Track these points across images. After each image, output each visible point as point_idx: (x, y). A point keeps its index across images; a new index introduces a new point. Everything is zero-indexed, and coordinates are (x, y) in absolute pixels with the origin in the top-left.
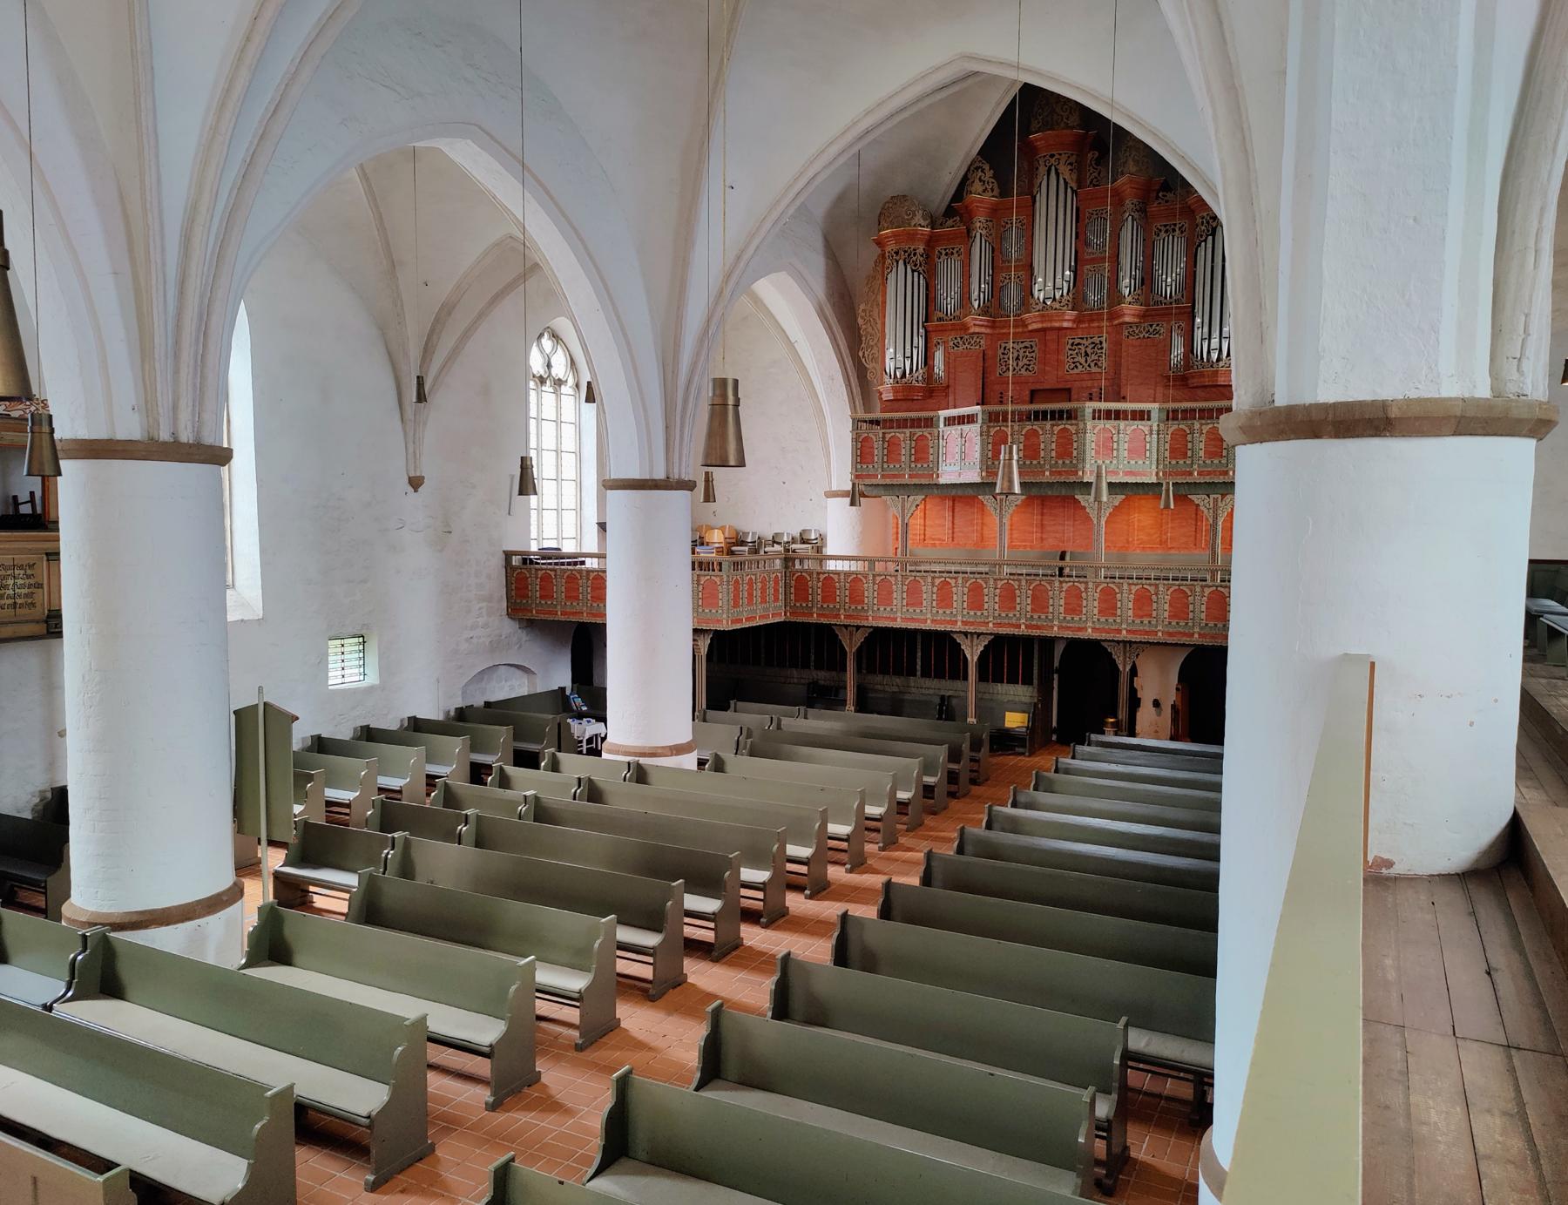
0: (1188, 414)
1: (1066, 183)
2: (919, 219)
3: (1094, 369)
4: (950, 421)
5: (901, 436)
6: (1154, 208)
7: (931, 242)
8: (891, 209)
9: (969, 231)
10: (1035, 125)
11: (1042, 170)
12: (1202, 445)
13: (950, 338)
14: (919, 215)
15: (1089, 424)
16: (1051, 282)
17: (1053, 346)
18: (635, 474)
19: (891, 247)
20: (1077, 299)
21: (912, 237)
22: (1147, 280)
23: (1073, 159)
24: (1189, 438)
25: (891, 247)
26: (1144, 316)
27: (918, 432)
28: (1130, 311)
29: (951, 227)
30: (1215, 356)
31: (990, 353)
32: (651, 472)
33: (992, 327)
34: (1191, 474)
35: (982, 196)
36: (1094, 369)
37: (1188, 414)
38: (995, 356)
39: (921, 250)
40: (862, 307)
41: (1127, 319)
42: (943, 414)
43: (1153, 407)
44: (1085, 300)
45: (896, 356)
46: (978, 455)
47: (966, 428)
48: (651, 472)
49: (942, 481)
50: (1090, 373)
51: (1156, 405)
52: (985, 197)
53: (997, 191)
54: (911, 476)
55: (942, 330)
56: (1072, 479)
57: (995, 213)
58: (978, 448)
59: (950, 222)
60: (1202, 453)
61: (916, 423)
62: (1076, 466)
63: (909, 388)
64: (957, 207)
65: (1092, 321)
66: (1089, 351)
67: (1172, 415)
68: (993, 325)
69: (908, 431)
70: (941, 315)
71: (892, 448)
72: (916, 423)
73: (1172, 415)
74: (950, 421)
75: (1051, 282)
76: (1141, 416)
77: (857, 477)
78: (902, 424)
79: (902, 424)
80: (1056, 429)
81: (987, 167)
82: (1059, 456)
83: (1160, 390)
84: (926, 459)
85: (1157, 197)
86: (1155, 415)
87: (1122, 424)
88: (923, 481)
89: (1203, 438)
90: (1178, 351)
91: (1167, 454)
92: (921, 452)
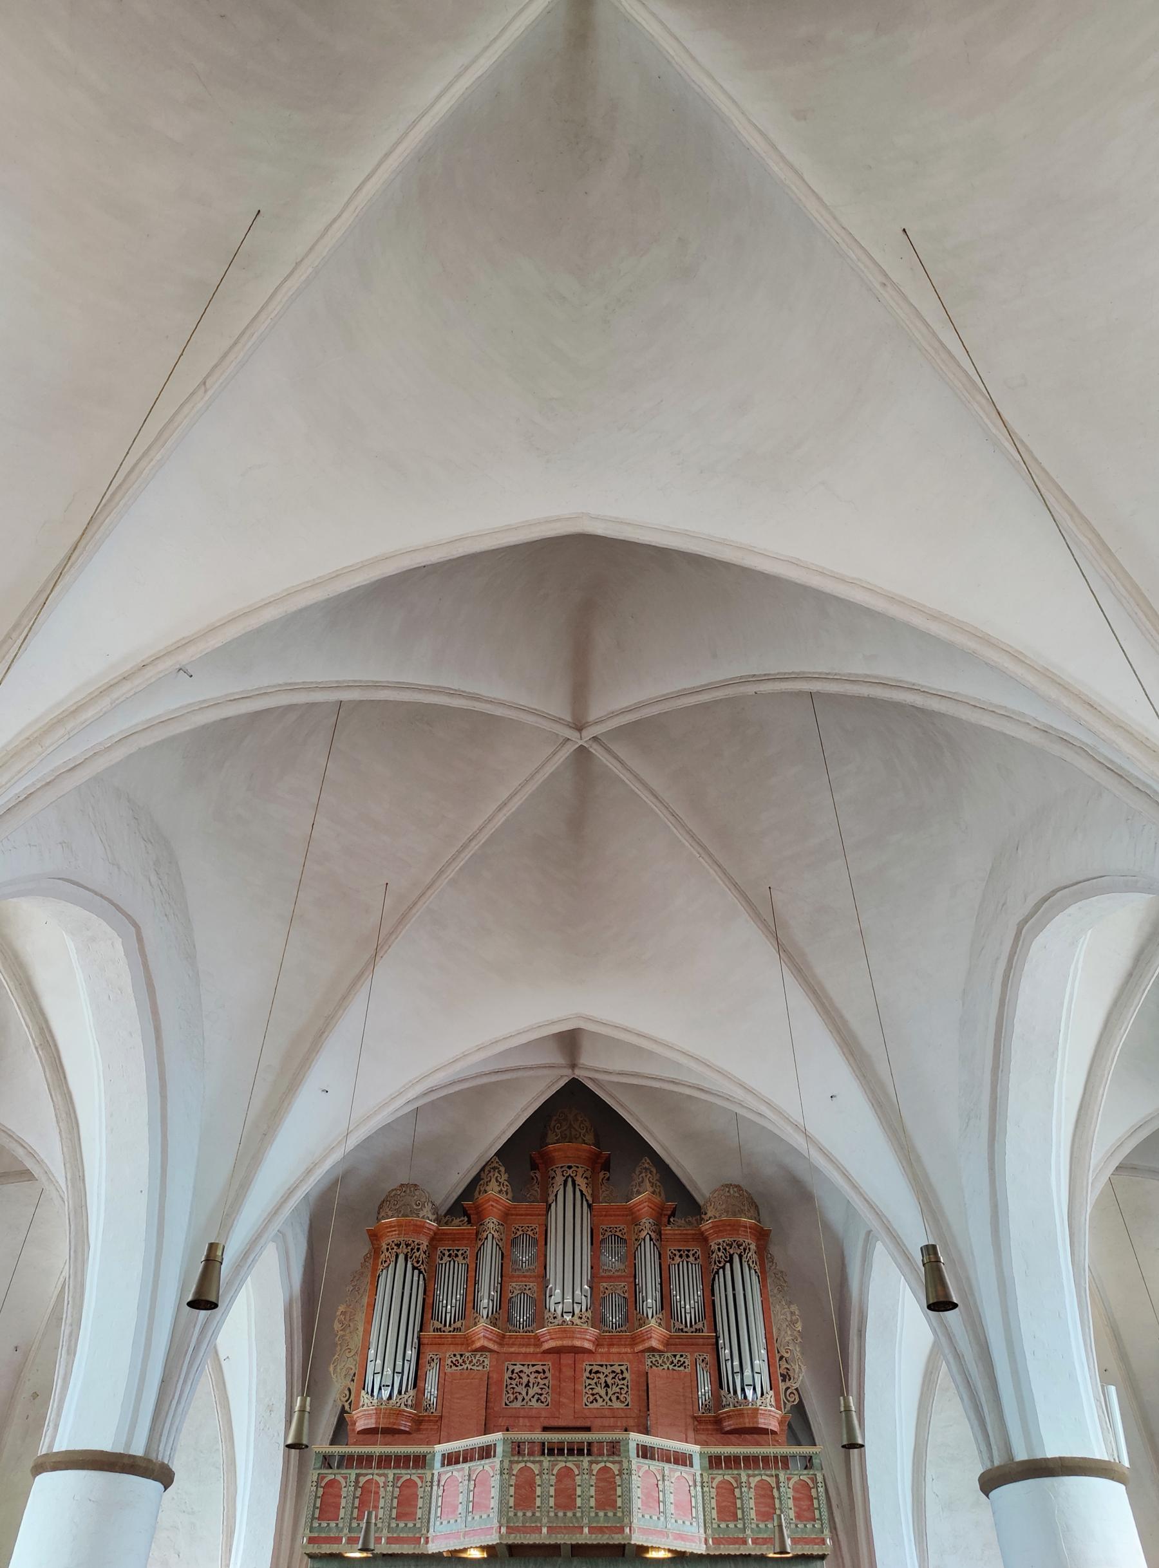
0: (732, 1462)
1: (582, 1194)
2: (427, 1212)
3: (616, 1405)
4: (451, 1459)
5: (381, 1480)
6: (668, 1230)
7: (436, 1239)
8: (398, 1199)
9: (477, 1233)
10: (551, 1137)
11: (559, 1180)
12: (752, 1503)
13: (448, 1354)
14: (428, 1207)
15: (636, 1462)
16: (567, 1296)
17: (568, 1372)
18: (105, 1442)
19: (391, 1238)
20: (598, 1320)
21: (418, 1229)
22: (665, 1301)
23: (588, 1174)
24: (737, 1491)
25: (391, 1238)
26: (668, 1343)
27: (406, 1474)
28: (655, 1331)
29: (457, 1225)
30: (749, 1393)
31: (495, 1376)
32: (128, 1444)
33: (501, 1344)
34: (745, 1542)
35: (496, 1193)
36: (616, 1405)
37: (732, 1462)
38: (501, 1381)
39: (424, 1247)
40: (341, 1308)
41: (654, 1343)
42: (441, 1448)
43: (694, 1449)
44: (603, 1320)
45: (381, 1372)
46: (494, 1503)
47: (477, 1466)
48: (128, 1444)
49: (432, 1548)
50: (611, 1409)
51: (697, 1448)
52: (503, 1197)
53: (509, 1196)
54: (390, 1541)
55: (438, 1343)
56: (617, 1539)
57: (506, 1217)
58: (495, 1493)
59: (457, 1221)
60: (753, 1514)
61: (403, 1461)
62: (621, 1520)
63: (399, 1413)
64: (466, 1206)
65: (611, 1345)
66: (610, 1381)
67: (714, 1462)
68: (501, 1340)
69: (390, 1473)
70: (438, 1325)
71: (366, 1497)
72: (403, 1461)
73: (714, 1462)
74: (451, 1459)
75: (567, 1296)
76: (682, 1459)
77: (311, 1540)
78: (385, 1461)
79: (385, 1461)
80: (596, 1468)
81: (502, 1169)
82: (601, 1505)
83: (691, 1434)
84: (411, 1516)
85: (669, 1222)
86: (696, 1461)
87: (667, 1467)
88: (407, 1549)
89: (752, 1494)
90: (705, 1389)
91: (714, 1514)
92: (407, 1504)
